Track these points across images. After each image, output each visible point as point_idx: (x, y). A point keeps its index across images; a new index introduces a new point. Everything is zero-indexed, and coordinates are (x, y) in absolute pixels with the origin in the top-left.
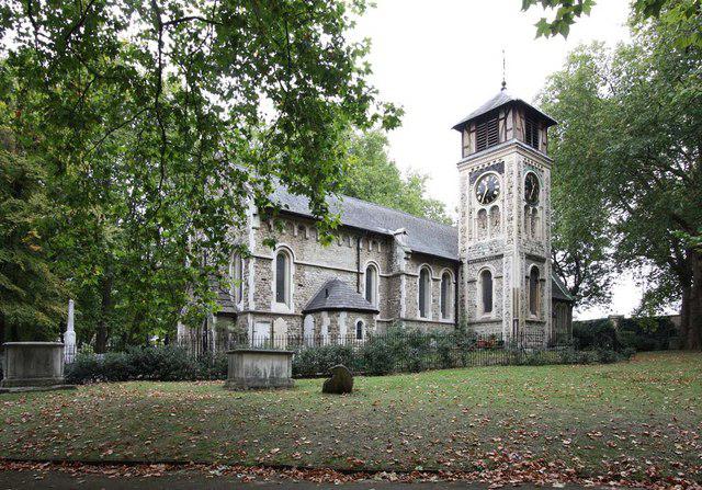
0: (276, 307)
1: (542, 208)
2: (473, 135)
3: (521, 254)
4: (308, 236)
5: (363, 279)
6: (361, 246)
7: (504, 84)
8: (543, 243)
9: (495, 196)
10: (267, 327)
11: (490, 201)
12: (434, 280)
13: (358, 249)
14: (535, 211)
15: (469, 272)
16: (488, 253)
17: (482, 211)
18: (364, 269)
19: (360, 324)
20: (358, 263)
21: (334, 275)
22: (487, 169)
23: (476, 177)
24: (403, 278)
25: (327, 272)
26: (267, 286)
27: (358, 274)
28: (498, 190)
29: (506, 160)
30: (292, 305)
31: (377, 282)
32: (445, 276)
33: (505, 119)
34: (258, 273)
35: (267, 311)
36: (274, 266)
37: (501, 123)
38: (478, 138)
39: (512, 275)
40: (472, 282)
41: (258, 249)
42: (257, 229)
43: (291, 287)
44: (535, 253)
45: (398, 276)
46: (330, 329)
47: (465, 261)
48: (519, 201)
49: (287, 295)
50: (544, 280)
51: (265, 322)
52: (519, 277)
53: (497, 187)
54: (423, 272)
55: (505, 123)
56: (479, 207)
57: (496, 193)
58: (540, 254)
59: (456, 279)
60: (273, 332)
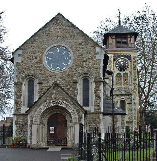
2: (114, 40)
9: (126, 69)
11: (124, 70)
22: (122, 56)
23: (116, 59)
28: (127, 66)
29: (132, 55)
38: (116, 42)
53: (127, 65)
55: (131, 40)
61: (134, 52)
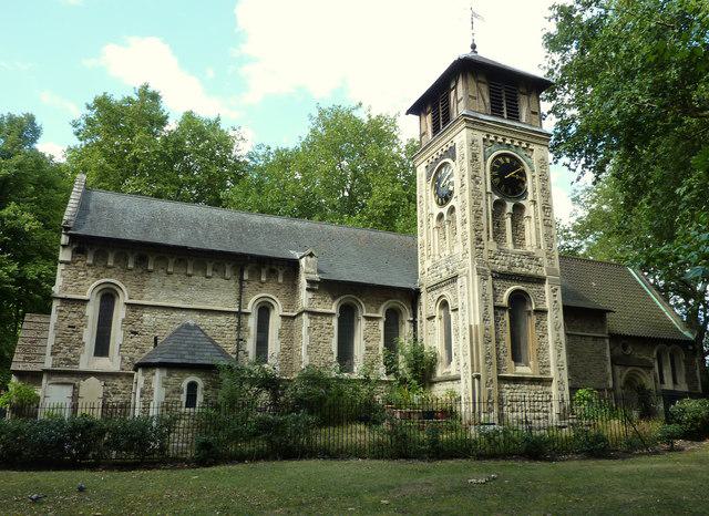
0: (88, 361)
1: (534, 202)
3: (482, 274)
4: (150, 267)
5: (252, 323)
6: (246, 277)
7: (474, 47)
8: (541, 254)
10: (68, 391)
12: (368, 318)
13: (241, 280)
14: (519, 209)
15: (428, 304)
16: (445, 275)
17: (441, 216)
18: (251, 306)
19: (192, 387)
20: (240, 299)
21: (192, 319)
26: (75, 336)
30: (117, 359)
31: (275, 322)
33: (455, 87)
34: (62, 319)
35: (74, 368)
36: (92, 311)
37: (453, 93)
39: (470, 304)
40: (431, 318)
41: (66, 289)
42: (67, 263)
43: (117, 335)
44: (518, 270)
46: (143, 392)
47: (423, 290)
48: (475, 194)
50: (544, 312)
51: (57, 384)
55: (456, 93)
56: (437, 210)
57: (451, 188)
60: (75, 397)
61: (457, 130)
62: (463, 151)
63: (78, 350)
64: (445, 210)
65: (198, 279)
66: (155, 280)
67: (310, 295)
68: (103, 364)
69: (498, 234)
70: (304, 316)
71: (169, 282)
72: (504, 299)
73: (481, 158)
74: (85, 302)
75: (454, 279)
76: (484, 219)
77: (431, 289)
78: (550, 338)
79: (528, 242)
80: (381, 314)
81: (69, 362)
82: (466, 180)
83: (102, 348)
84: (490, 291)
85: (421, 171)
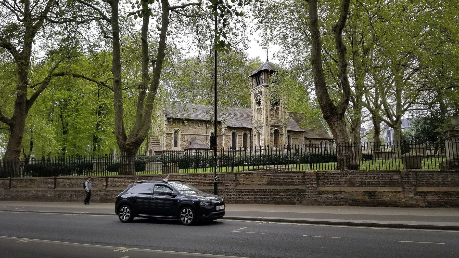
0: (174, 149)
6: (208, 126)
7: (267, 59)
12: (239, 136)
13: (207, 127)
14: (277, 109)
15: (254, 132)
16: (259, 125)
17: (258, 109)
21: (197, 137)
24: (224, 136)
25: (193, 136)
27: (207, 136)
29: (262, 91)
30: (180, 148)
32: (245, 135)
36: (173, 136)
40: (255, 136)
44: (276, 124)
45: (222, 135)
48: (266, 106)
49: (178, 145)
50: (283, 134)
52: (266, 134)
54: (234, 134)
56: (257, 107)
58: (280, 124)
59: (251, 135)
62: (263, 94)
63: (171, 146)
64: (259, 108)
65: (197, 127)
66: (187, 128)
67: (225, 130)
68: (176, 149)
69: (272, 115)
70: (224, 136)
71: (190, 128)
72: (273, 132)
73: (268, 96)
74: (171, 134)
75: (261, 127)
76: (268, 112)
77: (255, 128)
78: (284, 141)
79: (279, 117)
80: (242, 135)
81: (170, 149)
82: (264, 102)
83: (176, 145)
84: (269, 130)
85: (253, 95)
